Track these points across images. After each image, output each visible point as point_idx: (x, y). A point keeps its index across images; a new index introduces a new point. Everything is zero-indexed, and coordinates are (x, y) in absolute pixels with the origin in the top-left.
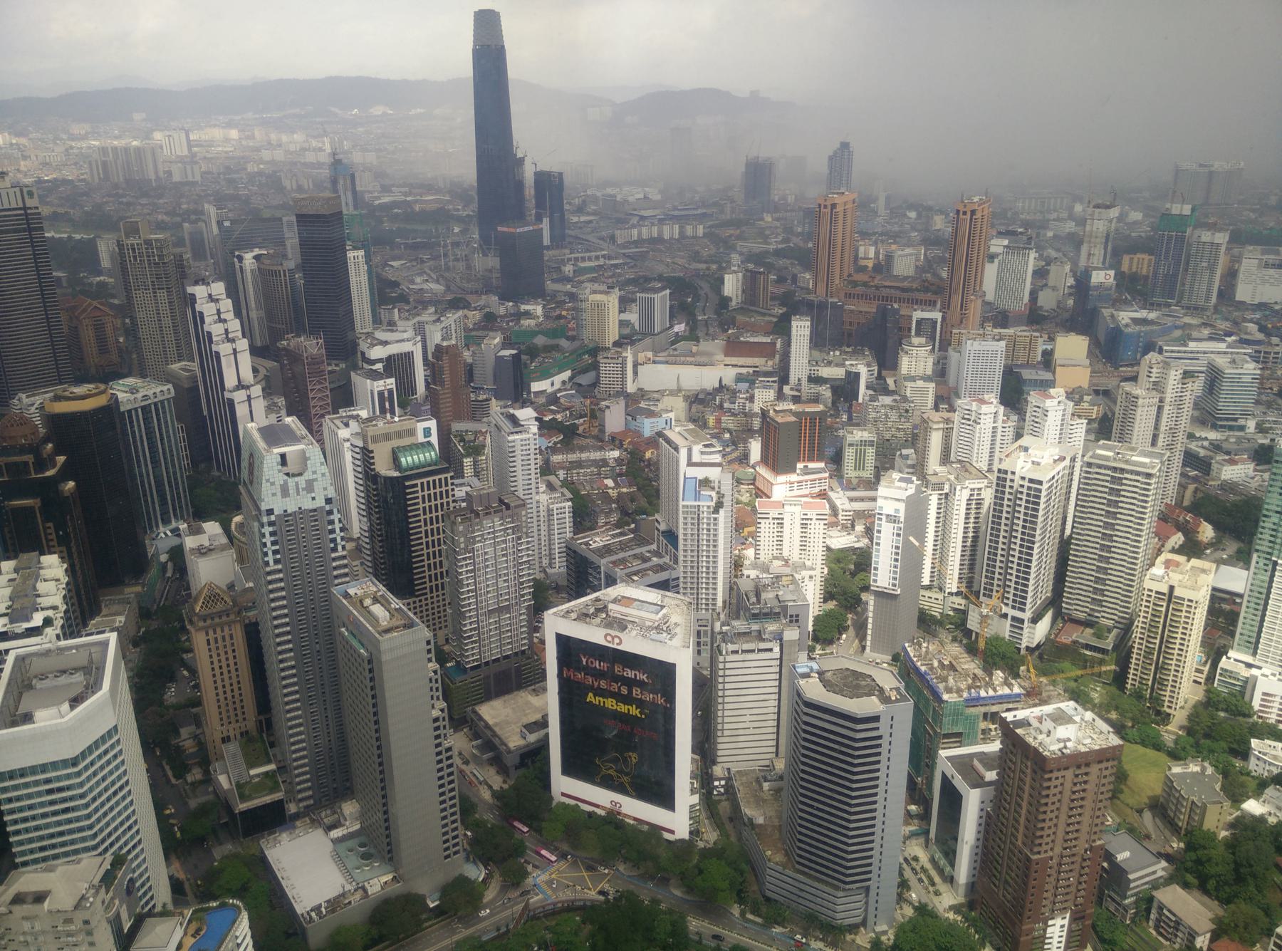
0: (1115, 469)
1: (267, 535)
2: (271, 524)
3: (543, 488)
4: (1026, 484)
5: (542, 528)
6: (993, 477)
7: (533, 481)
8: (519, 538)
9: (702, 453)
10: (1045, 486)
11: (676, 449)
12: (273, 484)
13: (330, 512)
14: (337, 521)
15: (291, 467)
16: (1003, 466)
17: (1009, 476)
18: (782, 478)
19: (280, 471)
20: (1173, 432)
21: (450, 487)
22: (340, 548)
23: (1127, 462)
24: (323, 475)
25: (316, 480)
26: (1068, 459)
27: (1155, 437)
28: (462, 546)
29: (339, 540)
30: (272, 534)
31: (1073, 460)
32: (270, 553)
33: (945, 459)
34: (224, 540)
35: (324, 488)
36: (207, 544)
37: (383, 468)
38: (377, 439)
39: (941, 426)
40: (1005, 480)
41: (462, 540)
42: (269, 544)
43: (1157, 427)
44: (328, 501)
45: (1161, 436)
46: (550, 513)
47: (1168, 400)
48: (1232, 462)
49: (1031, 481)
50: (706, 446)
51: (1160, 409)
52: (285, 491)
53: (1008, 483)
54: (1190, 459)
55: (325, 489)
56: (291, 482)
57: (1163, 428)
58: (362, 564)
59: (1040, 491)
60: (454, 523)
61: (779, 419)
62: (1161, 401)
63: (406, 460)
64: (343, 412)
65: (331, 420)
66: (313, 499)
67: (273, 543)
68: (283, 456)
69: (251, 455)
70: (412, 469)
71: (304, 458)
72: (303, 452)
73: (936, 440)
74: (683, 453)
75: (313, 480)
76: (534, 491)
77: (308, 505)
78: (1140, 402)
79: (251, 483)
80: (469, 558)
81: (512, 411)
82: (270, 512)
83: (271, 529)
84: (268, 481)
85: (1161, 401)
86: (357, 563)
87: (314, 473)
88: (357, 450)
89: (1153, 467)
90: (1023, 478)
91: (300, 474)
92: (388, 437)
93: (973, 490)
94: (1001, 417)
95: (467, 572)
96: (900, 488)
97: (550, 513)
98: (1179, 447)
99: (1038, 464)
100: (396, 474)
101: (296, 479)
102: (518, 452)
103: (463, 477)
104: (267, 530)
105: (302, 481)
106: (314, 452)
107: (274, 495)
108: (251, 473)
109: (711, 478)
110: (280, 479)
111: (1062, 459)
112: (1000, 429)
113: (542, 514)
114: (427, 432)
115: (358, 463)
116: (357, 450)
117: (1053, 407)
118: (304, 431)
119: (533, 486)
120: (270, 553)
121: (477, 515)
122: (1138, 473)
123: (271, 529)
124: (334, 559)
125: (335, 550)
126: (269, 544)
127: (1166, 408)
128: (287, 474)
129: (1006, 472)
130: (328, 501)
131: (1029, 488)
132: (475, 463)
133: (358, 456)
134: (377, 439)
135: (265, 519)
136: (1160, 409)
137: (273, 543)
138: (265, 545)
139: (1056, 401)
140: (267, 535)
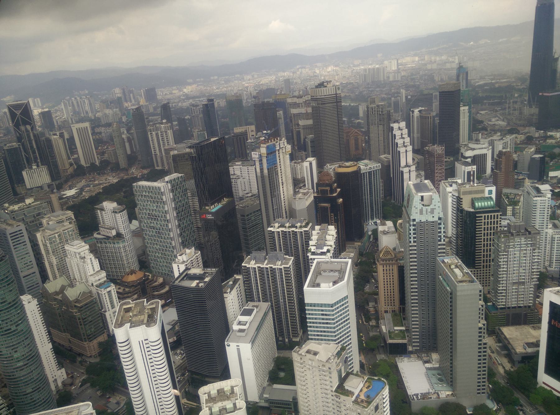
1: (412, 230)
2: (414, 225)
3: (550, 226)
5: (547, 246)
7: (545, 222)
8: (534, 250)
12: (417, 208)
13: (440, 224)
14: (442, 228)
15: (425, 202)
19: (420, 203)
21: (499, 220)
22: (442, 240)
24: (439, 207)
25: (435, 209)
28: (503, 248)
29: (442, 236)
30: (414, 230)
32: (412, 238)
34: (393, 229)
35: (438, 213)
36: (387, 230)
37: (467, 206)
38: (465, 193)
41: (503, 246)
42: (412, 234)
44: (440, 219)
46: (553, 239)
52: (421, 212)
55: (439, 213)
56: (424, 208)
58: (451, 249)
60: (499, 237)
63: (478, 204)
64: (449, 180)
65: (444, 183)
66: (433, 217)
67: (414, 234)
68: (422, 197)
69: (409, 195)
70: (480, 209)
71: (431, 199)
72: (431, 196)
75: (434, 209)
76: (545, 227)
77: (431, 219)
79: (408, 207)
80: (506, 255)
81: (537, 185)
82: (414, 220)
83: (414, 227)
84: (415, 207)
86: (449, 248)
87: (435, 205)
88: (455, 197)
91: (429, 206)
92: (470, 193)
95: (503, 261)
97: (553, 239)
100: (472, 210)
101: (427, 207)
102: (538, 206)
103: (506, 215)
104: (412, 228)
105: (429, 208)
106: (436, 196)
107: (417, 213)
108: (408, 203)
110: (420, 206)
113: (548, 239)
114: (490, 192)
115: (455, 203)
116: (455, 197)
118: (433, 187)
119: (545, 224)
120: (412, 238)
121: (512, 235)
123: (414, 227)
124: (439, 245)
125: (440, 241)
126: (412, 234)
128: (423, 205)
130: (440, 219)
132: (513, 209)
133: (455, 200)
134: (465, 193)
135: (412, 223)
137: (414, 234)
138: (410, 234)
140: (412, 230)
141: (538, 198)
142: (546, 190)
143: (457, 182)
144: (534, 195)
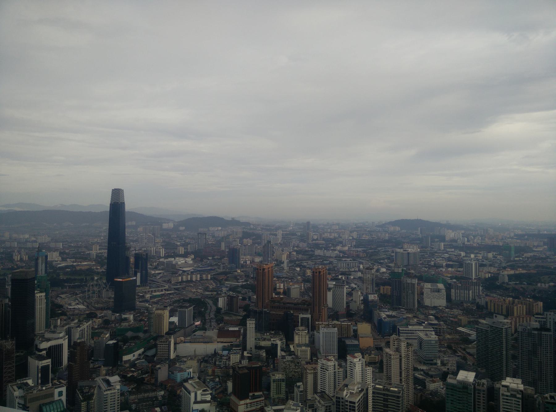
0: (384, 395)
4: (348, 404)
6: (334, 400)
9: (202, 395)
10: (357, 405)
11: (189, 393)
16: (338, 396)
17: (341, 400)
18: (242, 402)
20: (407, 369)
23: (389, 390)
26: (365, 390)
27: (401, 373)
31: (367, 390)
33: (315, 392)
39: (312, 371)
40: (339, 402)
43: (401, 369)
45: (403, 372)
47: (403, 356)
48: (434, 382)
49: (351, 402)
50: (204, 391)
51: (401, 360)
53: (341, 404)
54: (417, 381)
57: (403, 369)
59: (354, 407)
61: (240, 372)
62: (400, 356)
73: (310, 378)
74: (193, 395)
78: (392, 357)
81: (107, 377)
85: (400, 356)
89: (399, 393)
90: (347, 401)
92: (37, 399)
93: (327, 407)
94: (337, 367)
96: (293, 409)
98: (411, 378)
99: (353, 393)
109: (206, 409)
111: (362, 390)
112: (337, 373)
114: (60, 394)
116: (21, 406)
117: (357, 362)
122: (394, 396)
127: (403, 359)
129: (339, 398)
131: (350, 406)
132: (88, 404)
136: (401, 360)
139: (358, 360)
141: (109, 392)
142: (116, 382)
143: (27, 383)
144: (104, 389)
